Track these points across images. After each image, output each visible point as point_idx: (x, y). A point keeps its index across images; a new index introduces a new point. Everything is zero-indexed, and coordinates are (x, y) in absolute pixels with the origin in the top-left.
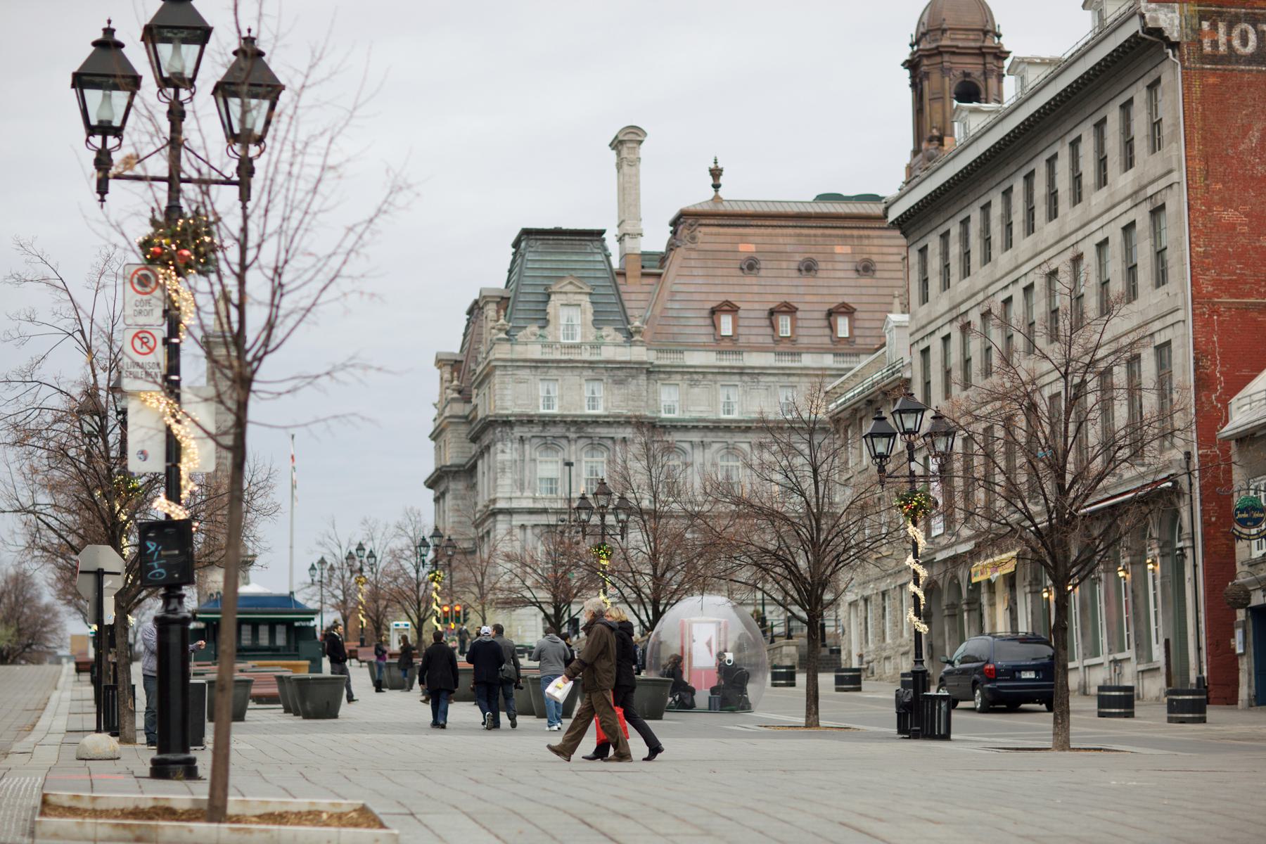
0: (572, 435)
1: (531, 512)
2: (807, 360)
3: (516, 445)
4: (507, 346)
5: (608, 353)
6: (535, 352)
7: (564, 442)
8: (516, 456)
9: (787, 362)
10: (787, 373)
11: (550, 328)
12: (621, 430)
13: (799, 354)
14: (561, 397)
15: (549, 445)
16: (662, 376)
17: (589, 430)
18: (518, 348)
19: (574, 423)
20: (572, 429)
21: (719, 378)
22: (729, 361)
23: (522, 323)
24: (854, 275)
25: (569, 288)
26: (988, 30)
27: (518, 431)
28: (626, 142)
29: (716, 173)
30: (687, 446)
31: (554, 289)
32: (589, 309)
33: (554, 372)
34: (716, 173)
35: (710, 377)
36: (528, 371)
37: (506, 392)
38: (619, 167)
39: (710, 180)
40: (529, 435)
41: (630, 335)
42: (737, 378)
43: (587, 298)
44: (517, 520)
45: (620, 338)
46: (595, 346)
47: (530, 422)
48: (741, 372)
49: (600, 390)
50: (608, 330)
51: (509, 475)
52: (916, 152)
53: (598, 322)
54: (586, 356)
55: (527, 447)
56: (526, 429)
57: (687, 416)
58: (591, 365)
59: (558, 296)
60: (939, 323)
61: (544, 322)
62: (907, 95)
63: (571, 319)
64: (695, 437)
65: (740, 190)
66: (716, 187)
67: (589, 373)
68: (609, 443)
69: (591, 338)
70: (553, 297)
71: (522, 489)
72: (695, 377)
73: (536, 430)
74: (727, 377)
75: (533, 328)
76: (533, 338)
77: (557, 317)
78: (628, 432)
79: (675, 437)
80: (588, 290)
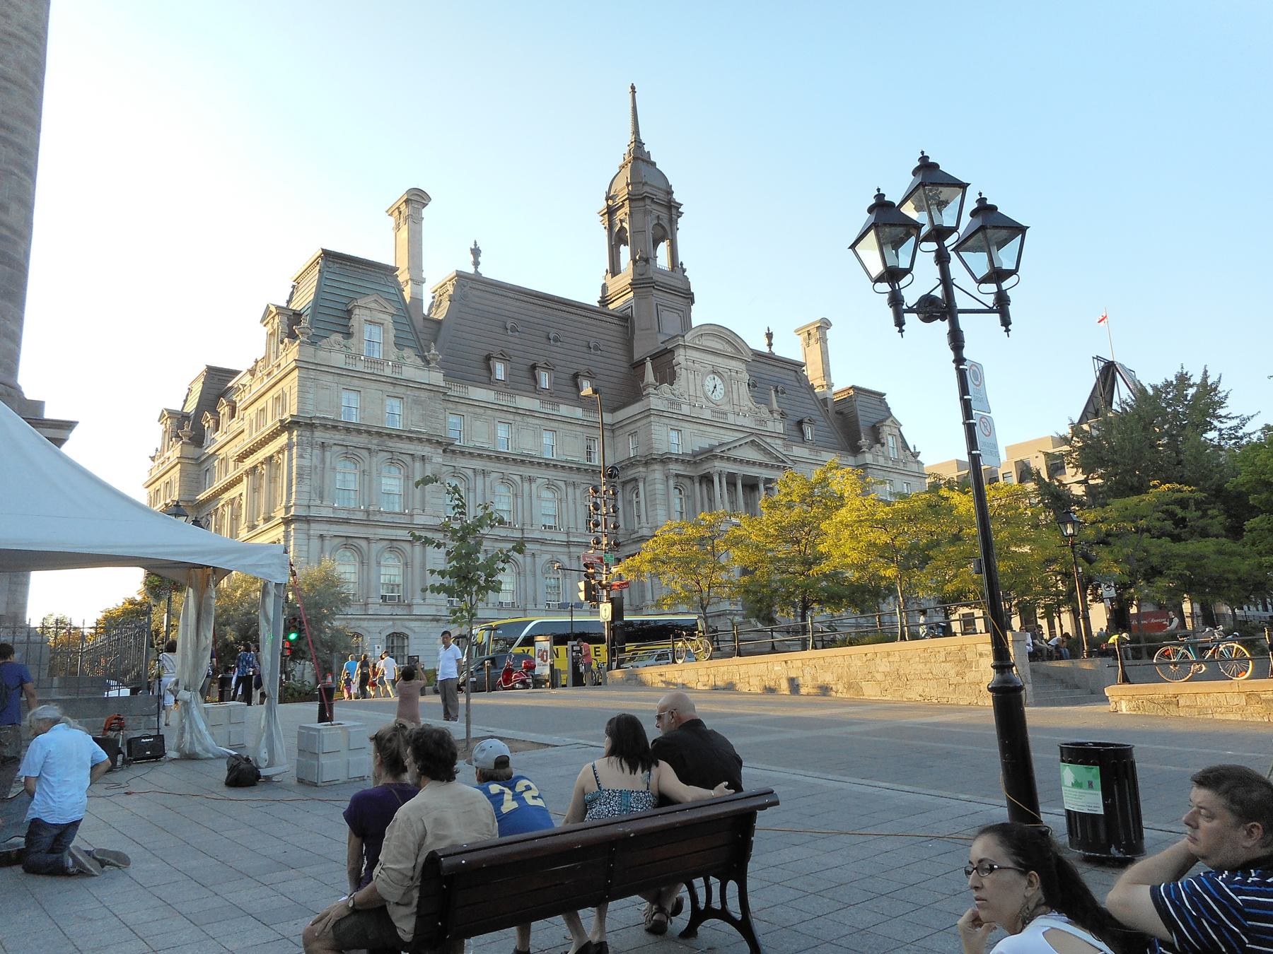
0: (373, 447)
1: (330, 521)
2: (564, 410)
3: (317, 452)
4: (311, 349)
5: (409, 372)
6: (338, 359)
7: (365, 453)
8: (316, 461)
11: (353, 341)
12: (419, 448)
13: (558, 404)
14: (362, 409)
15: (350, 454)
16: (450, 405)
17: (390, 444)
18: (320, 353)
19: (379, 433)
20: (375, 441)
21: (498, 414)
22: (505, 400)
23: (322, 333)
24: (585, 349)
25: (373, 305)
26: (670, 192)
27: (319, 435)
28: (417, 199)
29: (476, 252)
30: (470, 473)
31: (360, 302)
32: (392, 333)
33: (356, 382)
34: (476, 252)
35: (489, 412)
36: (330, 377)
37: (308, 396)
38: (398, 228)
39: (471, 258)
40: (332, 442)
41: (427, 362)
42: (511, 417)
43: (389, 318)
44: (316, 529)
45: (419, 361)
46: (398, 365)
47: (335, 427)
48: (517, 412)
49: (394, 406)
50: (408, 353)
51: (307, 481)
52: (614, 270)
53: (398, 345)
54: (388, 372)
55: (328, 454)
56: (328, 436)
57: (471, 444)
58: (395, 382)
59: (363, 311)
61: (348, 335)
62: (605, 234)
63: (374, 334)
64: (478, 464)
67: (390, 388)
68: (408, 459)
69: (393, 357)
70: (357, 311)
71: (322, 498)
72: (477, 410)
73: (338, 437)
74: (503, 415)
75: (338, 337)
76: (337, 347)
77: (361, 331)
78: (426, 450)
79: (461, 462)
80: (392, 311)
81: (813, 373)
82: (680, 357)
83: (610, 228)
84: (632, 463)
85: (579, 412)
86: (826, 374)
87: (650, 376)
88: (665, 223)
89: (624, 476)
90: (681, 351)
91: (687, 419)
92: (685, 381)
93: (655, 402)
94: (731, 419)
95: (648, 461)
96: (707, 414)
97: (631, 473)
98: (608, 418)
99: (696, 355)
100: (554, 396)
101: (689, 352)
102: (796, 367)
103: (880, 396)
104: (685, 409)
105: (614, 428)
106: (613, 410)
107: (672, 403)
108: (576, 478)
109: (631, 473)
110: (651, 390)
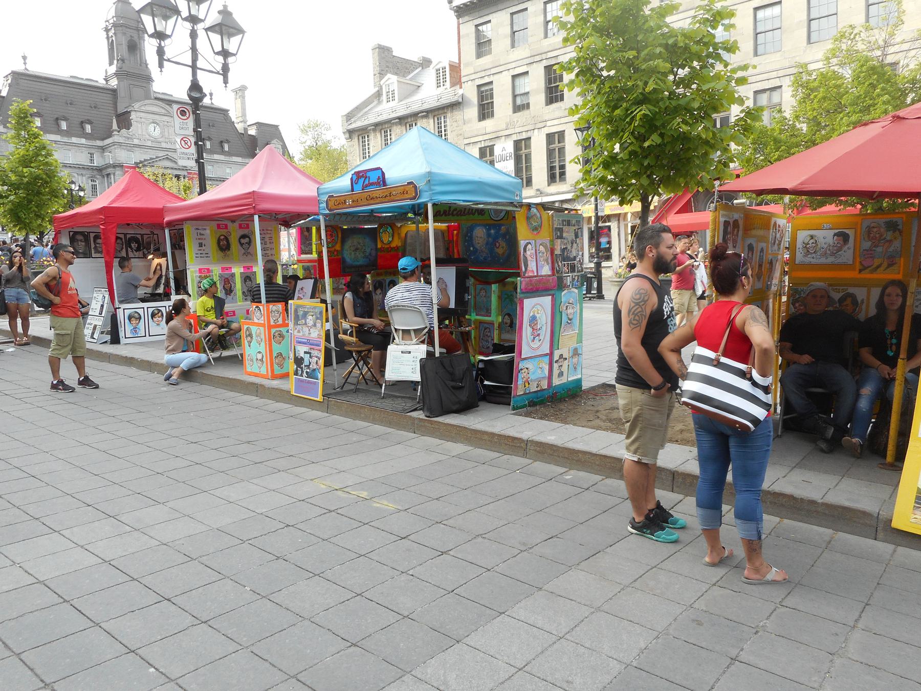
9: (65, 139)
10: (66, 144)
29: (24, 58)
34: (24, 58)
52: (111, 64)
60: (513, 65)
65: (37, 67)
66: (25, 63)
81: (234, 115)
82: (133, 116)
83: (108, 38)
84: (108, 166)
85: (83, 141)
86: (244, 114)
87: (115, 126)
88: (136, 38)
89: (105, 172)
90: (132, 113)
91: (139, 146)
92: (136, 128)
93: (116, 138)
94: (164, 145)
95: (114, 166)
96: (149, 144)
97: (110, 170)
98: (99, 143)
99: (142, 115)
100: (68, 133)
101: (138, 114)
102: (224, 112)
103: (276, 127)
104: (136, 142)
105: (103, 149)
106: (103, 139)
107: (128, 138)
108: (84, 172)
109: (110, 170)
110: (115, 133)
